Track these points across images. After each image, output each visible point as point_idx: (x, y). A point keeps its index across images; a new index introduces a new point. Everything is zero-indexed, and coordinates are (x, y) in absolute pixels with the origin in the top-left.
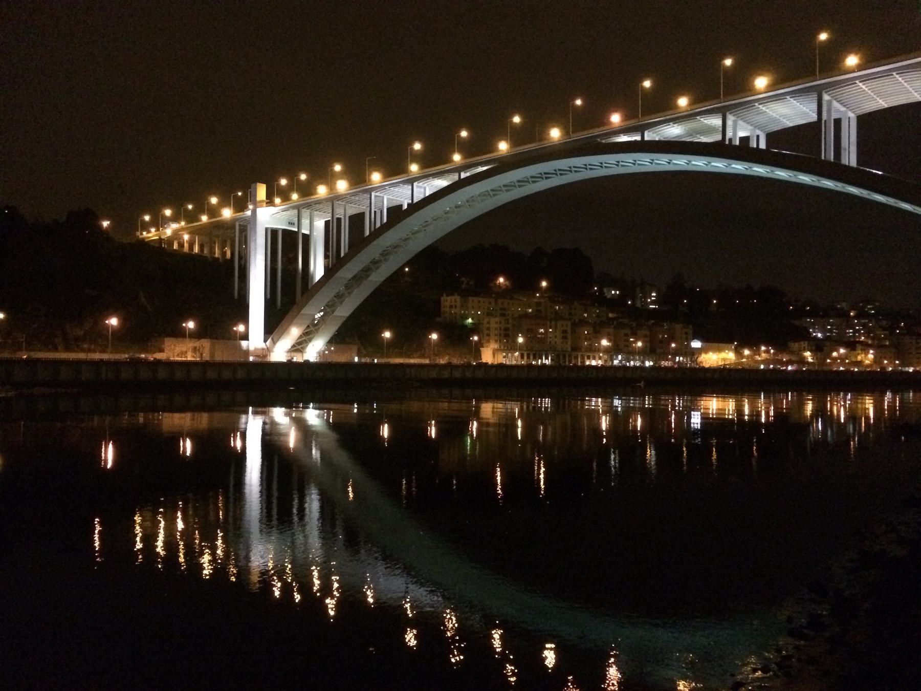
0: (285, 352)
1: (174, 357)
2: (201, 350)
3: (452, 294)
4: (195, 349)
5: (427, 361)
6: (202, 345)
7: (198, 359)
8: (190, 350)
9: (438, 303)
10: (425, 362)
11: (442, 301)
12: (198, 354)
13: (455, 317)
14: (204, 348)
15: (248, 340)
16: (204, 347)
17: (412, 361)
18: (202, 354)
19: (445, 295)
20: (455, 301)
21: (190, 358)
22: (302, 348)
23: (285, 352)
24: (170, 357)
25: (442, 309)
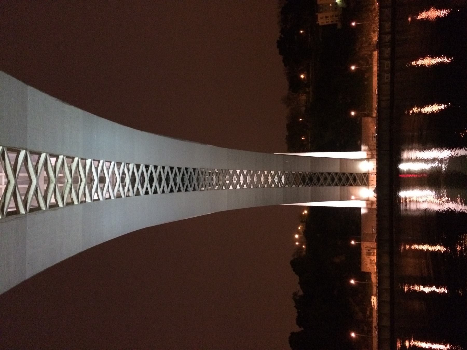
0: (369, 188)
1: (374, 269)
2: (369, 249)
3: (317, 17)
4: (369, 254)
5: (376, 53)
6: (365, 248)
7: (375, 251)
8: (369, 256)
9: (325, 27)
10: (377, 55)
11: (323, 24)
12: (371, 252)
13: (336, 16)
14: (367, 247)
15: (360, 208)
16: (367, 246)
17: (375, 68)
18: (372, 248)
19: (317, 23)
20: (322, 18)
21: (375, 258)
22: (365, 176)
23: (369, 188)
24: (374, 272)
25: (330, 23)
